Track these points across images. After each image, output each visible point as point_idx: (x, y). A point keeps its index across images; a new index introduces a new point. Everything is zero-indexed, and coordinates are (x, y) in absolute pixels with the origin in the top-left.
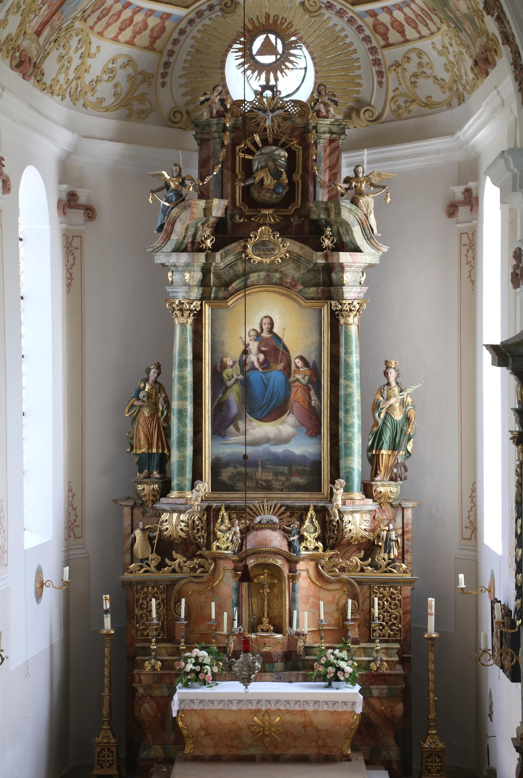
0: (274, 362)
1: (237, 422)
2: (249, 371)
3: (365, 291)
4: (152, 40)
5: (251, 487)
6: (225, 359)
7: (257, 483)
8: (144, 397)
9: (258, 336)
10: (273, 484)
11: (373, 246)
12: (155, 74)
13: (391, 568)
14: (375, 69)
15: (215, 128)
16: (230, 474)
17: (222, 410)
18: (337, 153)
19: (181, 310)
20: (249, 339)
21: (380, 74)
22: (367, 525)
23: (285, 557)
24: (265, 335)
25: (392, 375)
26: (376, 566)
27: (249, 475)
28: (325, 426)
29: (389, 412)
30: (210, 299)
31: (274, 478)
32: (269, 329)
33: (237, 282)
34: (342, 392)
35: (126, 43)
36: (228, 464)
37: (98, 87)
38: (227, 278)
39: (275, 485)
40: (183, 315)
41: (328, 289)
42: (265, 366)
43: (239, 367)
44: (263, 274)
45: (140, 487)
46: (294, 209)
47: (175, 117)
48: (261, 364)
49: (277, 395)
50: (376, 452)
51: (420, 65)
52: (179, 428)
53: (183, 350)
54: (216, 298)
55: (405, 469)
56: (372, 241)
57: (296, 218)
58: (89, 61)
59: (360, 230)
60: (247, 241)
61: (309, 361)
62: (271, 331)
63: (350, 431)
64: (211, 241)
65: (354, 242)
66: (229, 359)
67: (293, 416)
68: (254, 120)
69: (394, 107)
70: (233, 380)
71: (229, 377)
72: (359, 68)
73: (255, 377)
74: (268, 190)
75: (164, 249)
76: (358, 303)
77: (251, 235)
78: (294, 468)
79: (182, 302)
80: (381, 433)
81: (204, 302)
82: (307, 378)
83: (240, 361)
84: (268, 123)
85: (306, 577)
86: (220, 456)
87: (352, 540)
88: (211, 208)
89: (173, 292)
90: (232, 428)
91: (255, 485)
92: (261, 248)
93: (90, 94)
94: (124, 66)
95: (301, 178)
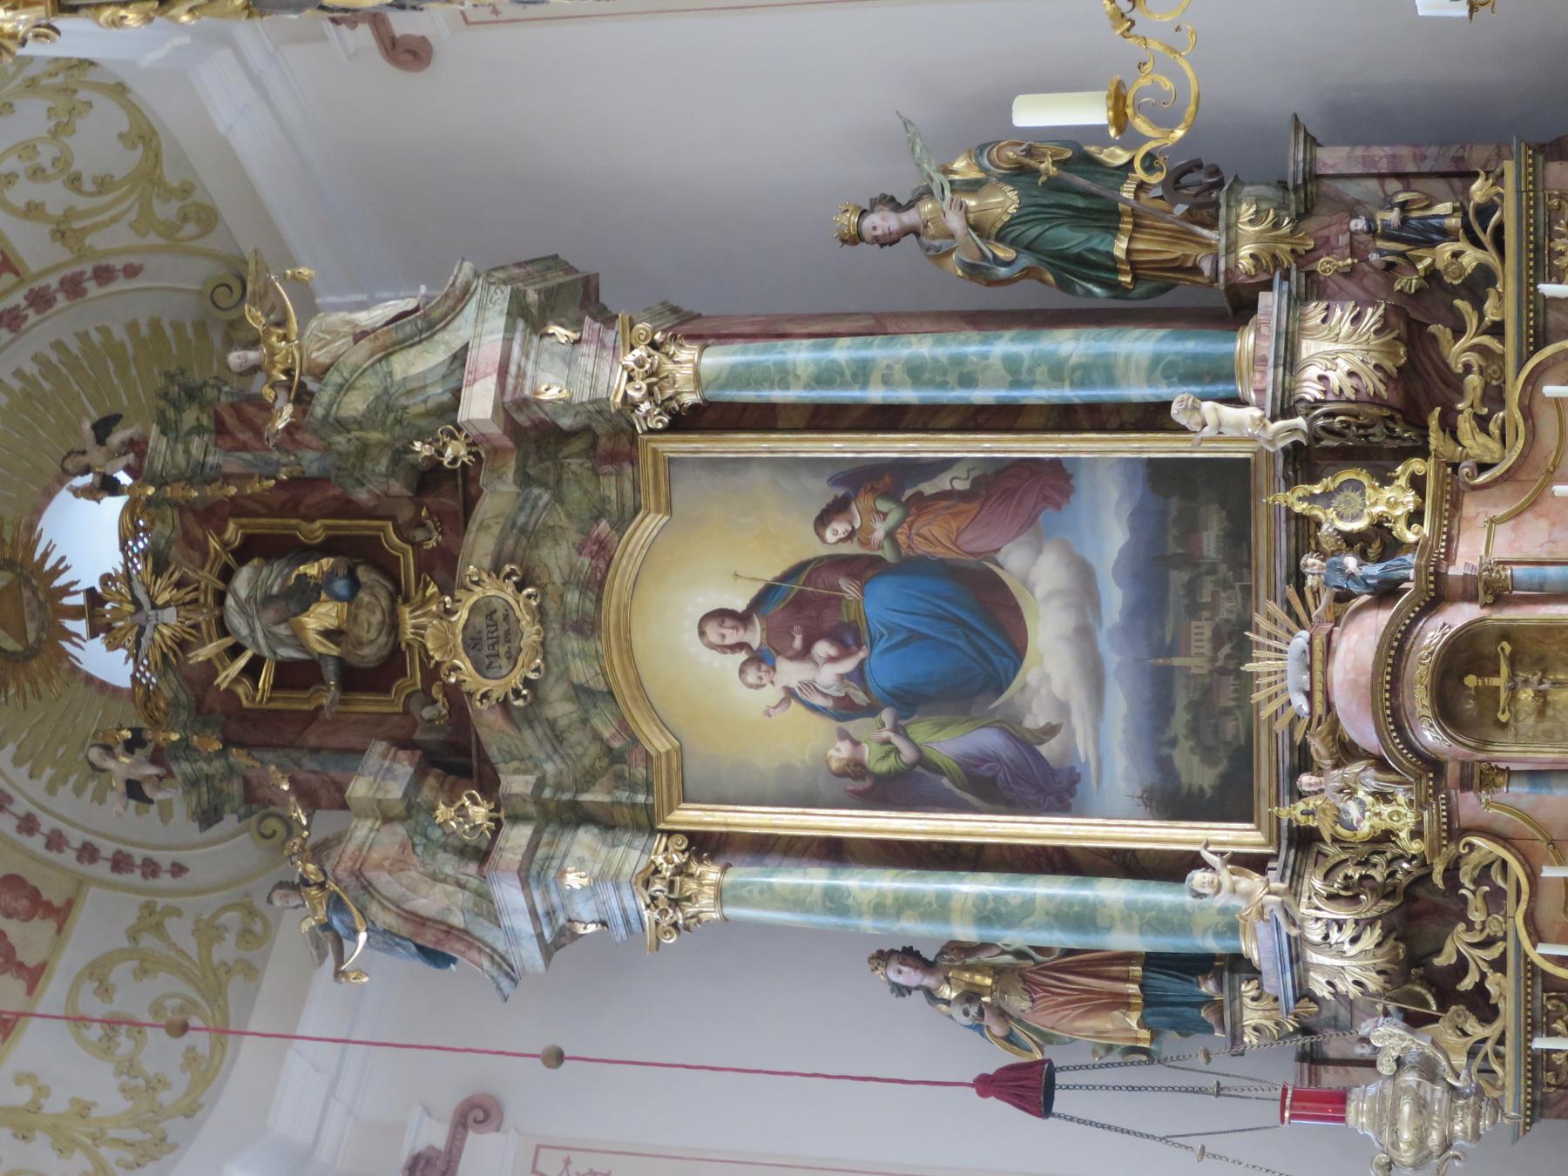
0: (838, 609)
1: (1029, 731)
2: (866, 692)
3: (597, 325)
4: (40, 913)
5: (1236, 690)
6: (834, 765)
7: (1223, 671)
8: (966, 1013)
9: (759, 659)
10: (1227, 621)
11: (453, 308)
12: (143, 899)
13: (1485, 231)
14: (93, 289)
15: (205, 767)
16: (1196, 759)
17: (992, 781)
18: (251, 411)
19: (675, 903)
20: (769, 686)
21: (104, 275)
22: (1338, 312)
23: (1415, 621)
24: (755, 636)
25: (882, 222)
26: (1479, 285)
27: (1196, 696)
28: (1029, 446)
29: (994, 231)
30: (653, 806)
31: (1206, 614)
32: (739, 625)
33: (597, 722)
34: (908, 395)
35: (31, 990)
36: (1164, 766)
37: (150, 1068)
38: (594, 750)
39: (1230, 611)
40: (688, 899)
41: (603, 442)
42: (850, 640)
43: (858, 722)
44: (573, 643)
45: (1250, 1038)
46: (397, 540)
47: (274, 832)
48: (845, 652)
49: (938, 602)
50: (1125, 273)
51: (37, 173)
52: (1035, 927)
53: (795, 901)
54: (649, 788)
55: (1190, 171)
56: (436, 314)
57: (419, 535)
58: (56, 1104)
59: (404, 352)
60: (470, 694)
61: (829, 499)
62: (743, 619)
63: (1031, 371)
64: (476, 803)
65: (443, 370)
66: (832, 753)
67: (1003, 551)
68: (171, 655)
69: (190, 229)
70: (898, 742)
71: (887, 755)
72: (105, 331)
73: (886, 674)
74: (353, 618)
75: (501, 946)
76: (632, 348)
77: (453, 680)
78: (1173, 548)
79: (648, 901)
80: (1063, 256)
81: (662, 826)
82: (883, 506)
83: (839, 718)
84: (170, 615)
85: (1514, 529)
86: (1139, 793)
87: (1388, 365)
88: (380, 801)
89: (627, 922)
90: (1049, 750)
91: (1231, 679)
92: (486, 651)
93: (165, 1097)
94: (105, 991)
95: (312, 520)
